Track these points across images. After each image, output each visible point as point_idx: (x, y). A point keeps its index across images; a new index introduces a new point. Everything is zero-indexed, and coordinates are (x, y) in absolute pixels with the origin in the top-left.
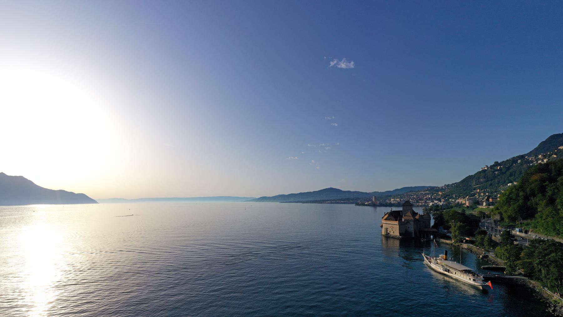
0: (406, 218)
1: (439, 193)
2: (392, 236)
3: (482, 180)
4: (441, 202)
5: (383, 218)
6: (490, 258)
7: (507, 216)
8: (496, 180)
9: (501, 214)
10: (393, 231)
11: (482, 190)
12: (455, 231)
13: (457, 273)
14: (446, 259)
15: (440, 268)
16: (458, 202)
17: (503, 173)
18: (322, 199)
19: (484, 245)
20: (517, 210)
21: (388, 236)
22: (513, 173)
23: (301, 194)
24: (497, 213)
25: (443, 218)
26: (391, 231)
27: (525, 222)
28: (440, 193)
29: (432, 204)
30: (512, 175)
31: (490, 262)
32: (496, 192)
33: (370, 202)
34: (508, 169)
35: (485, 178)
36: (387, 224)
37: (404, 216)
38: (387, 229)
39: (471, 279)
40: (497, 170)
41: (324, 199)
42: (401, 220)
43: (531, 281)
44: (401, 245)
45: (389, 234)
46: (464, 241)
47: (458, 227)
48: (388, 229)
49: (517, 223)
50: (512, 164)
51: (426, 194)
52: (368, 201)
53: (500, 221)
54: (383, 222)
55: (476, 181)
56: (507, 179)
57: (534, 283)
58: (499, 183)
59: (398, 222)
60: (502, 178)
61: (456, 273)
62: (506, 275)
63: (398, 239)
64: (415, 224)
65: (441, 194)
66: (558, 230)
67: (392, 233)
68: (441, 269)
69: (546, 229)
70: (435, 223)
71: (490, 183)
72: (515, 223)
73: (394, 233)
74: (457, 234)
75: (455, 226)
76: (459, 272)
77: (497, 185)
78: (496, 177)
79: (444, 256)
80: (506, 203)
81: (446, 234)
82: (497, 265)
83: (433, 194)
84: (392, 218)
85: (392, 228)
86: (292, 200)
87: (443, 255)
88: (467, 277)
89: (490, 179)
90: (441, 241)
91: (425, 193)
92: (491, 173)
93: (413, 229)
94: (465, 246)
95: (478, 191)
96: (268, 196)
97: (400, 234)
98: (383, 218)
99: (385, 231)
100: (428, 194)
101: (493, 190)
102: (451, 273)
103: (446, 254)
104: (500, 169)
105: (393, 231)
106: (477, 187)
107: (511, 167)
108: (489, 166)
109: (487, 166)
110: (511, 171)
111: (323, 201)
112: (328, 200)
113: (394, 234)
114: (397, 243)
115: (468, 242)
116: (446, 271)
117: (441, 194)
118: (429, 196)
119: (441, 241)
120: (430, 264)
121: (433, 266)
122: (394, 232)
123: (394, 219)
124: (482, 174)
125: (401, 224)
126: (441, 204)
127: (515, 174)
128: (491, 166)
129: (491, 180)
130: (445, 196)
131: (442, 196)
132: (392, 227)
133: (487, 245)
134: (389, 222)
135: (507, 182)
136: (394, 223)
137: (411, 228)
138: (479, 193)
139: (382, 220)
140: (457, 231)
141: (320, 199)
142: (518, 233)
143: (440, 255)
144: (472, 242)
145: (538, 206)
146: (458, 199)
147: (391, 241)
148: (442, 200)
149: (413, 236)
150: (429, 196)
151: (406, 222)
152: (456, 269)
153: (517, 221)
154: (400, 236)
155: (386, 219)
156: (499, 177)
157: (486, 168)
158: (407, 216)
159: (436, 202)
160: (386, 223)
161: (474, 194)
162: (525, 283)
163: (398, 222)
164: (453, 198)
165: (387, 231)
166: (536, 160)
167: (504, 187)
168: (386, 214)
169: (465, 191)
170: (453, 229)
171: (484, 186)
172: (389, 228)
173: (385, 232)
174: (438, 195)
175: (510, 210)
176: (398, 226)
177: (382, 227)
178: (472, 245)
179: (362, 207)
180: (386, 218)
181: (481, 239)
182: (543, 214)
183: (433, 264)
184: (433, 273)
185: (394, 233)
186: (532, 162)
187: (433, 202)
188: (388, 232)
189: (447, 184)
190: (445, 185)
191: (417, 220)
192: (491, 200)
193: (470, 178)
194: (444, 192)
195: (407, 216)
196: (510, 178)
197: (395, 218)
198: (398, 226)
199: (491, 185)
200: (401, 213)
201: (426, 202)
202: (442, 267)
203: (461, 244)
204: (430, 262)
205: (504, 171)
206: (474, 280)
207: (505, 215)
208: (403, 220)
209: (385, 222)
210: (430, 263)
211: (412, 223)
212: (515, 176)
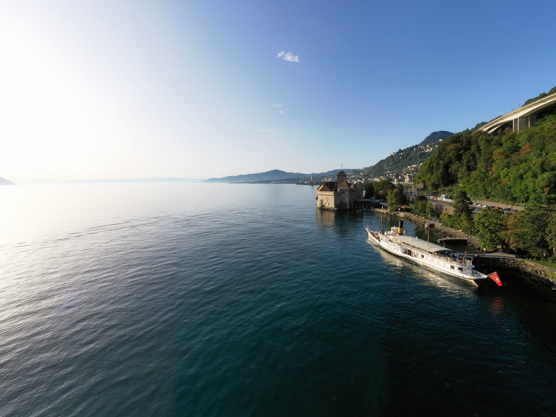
0: (342, 188)
1: (361, 174)
2: (327, 208)
3: (390, 163)
4: (362, 181)
5: (318, 189)
6: (437, 227)
7: (431, 184)
8: (400, 164)
9: (424, 182)
10: (328, 203)
11: (391, 171)
12: (392, 199)
13: (425, 257)
14: (401, 234)
15: (396, 248)
16: (375, 180)
17: (404, 158)
18: (267, 180)
19: (425, 213)
20: (440, 177)
21: (323, 209)
22: (411, 159)
23: (249, 175)
24: (421, 181)
25: (373, 189)
26: (327, 204)
27: (447, 188)
28: (361, 174)
29: (356, 183)
30: (411, 159)
31: (439, 232)
32: (400, 173)
33: (309, 181)
34: (408, 155)
35: (393, 162)
36: (322, 195)
37: (340, 186)
38: (322, 200)
39: (455, 267)
40: (401, 156)
41: (270, 180)
42: (337, 190)
43: (526, 261)
44: (336, 218)
45: (324, 206)
46: (399, 209)
47: (395, 194)
48: (323, 201)
49: (439, 190)
50: (410, 152)
51: (351, 175)
52: (307, 181)
53: (423, 189)
54: (318, 193)
55: (386, 164)
56: (407, 163)
57: (534, 265)
58: (402, 166)
59: (333, 192)
60: (404, 162)
61: (423, 256)
62: (485, 253)
63: (333, 211)
64: (350, 194)
65: (362, 174)
66: (490, 193)
67: (327, 206)
68: (399, 249)
69: (475, 193)
70: (366, 195)
71: (396, 165)
72: (438, 190)
73: (329, 205)
74: (393, 201)
75: (392, 193)
76: (430, 255)
77: (400, 168)
78: (400, 161)
79: (399, 229)
80: (428, 172)
81: (379, 204)
82: (451, 236)
83: (356, 175)
84: (327, 188)
85: (327, 199)
86: (240, 181)
87: (396, 228)
88: (439, 261)
89: (396, 163)
90: (376, 211)
91: (351, 174)
92: (397, 158)
93: (348, 200)
94: (402, 214)
95: (388, 172)
96: (217, 178)
97: (335, 205)
98: (318, 189)
99: (320, 203)
100: (353, 175)
101: (398, 172)
102: (415, 256)
103: (401, 227)
104: (403, 155)
105: (328, 203)
106: (387, 169)
107: (410, 154)
108: (395, 153)
109: (394, 152)
110: (410, 156)
111: (268, 181)
112: (273, 181)
113: (329, 206)
114: (332, 215)
115: (403, 210)
116: (405, 253)
117: (362, 174)
118: (354, 176)
119: (376, 211)
120: (379, 242)
121: (384, 244)
123: (329, 190)
124: (391, 159)
125: (336, 195)
126: (363, 182)
127: (412, 159)
128: (396, 152)
129: (397, 163)
130: (366, 176)
131: (363, 176)
132: (328, 198)
133: (429, 212)
134: (324, 193)
135: (407, 165)
136: (329, 194)
137: (347, 199)
138: (389, 174)
139: (318, 191)
140: (394, 199)
141: (265, 180)
142: (444, 199)
143: (392, 228)
144: (408, 210)
145: (459, 172)
146: (374, 178)
147: (327, 213)
148: (363, 179)
149: (348, 207)
150: (354, 176)
151: (341, 192)
152: (408, 244)
153: (439, 188)
154: (335, 207)
155: (321, 190)
156: (402, 161)
157: (393, 154)
158: (343, 186)
159: (359, 181)
160: (322, 194)
161: (386, 175)
162: (518, 265)
163: (333, 192)
164: (371, 178)
165: (322, 203)
166: (425, 149)
167: (405, 169)
168: (322, 185)
169: (379, 172)
170: (390, 197)
171: (392, 168)
173: (320, 205)
174: (360, 175)
175: (434, 177)
176: (334, 196)
177: (317, 199)
178: (408, 213)
179: (302, 185)
180: (321, 189)
181: (422, 205)
182: (471, 178)
183: (384, 242)
184: (383, 253)
185: (329, 205)
186: (423, 150)
187: (357, 181)
188: (324, 204)
189: (366, 167)
190: (365, 168)
191: (352, 190)
192: (400, 177)
193: (382, 161)
194: (364, 172)
195: (343, 186)
196: (409, 162)
197: (330, 189)
198: (333, 197)
199: (397, 167)
200: (335, 184)
201: (351, 181)
202: (399, 247)
203: (398, 213)
204: (378, 238)
205: (405, 157)
206: (460, 269)
207: (428, 184)
208: (338, 190)
209: (320, 193)
210: (379, 241)
211: (347, 193)
212: (412, 160)
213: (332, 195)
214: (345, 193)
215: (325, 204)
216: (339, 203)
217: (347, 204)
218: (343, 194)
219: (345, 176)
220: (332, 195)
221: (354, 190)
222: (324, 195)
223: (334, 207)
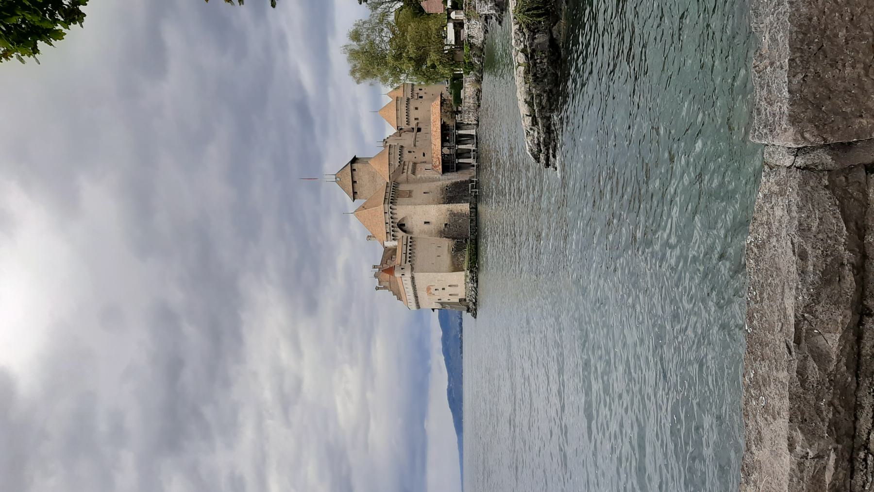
10: (447, 288)
64: (410, 194)
85: (433, 291)
97: (456, 268)
105: (447, 288)
122: (449, 286)
132: (428, 289)
151: (400, 234)
172: (439, 298)
211: (402, 211)
213: (413, 278)
214: (403, 219)
215: (456, 295)
216: (447, 244)
217: (453, 214)
218: (408, 225)
219: (353, 170)
220: (413, 278)
221: (397, 164)
222: (416, 297)
223: (463, 273)
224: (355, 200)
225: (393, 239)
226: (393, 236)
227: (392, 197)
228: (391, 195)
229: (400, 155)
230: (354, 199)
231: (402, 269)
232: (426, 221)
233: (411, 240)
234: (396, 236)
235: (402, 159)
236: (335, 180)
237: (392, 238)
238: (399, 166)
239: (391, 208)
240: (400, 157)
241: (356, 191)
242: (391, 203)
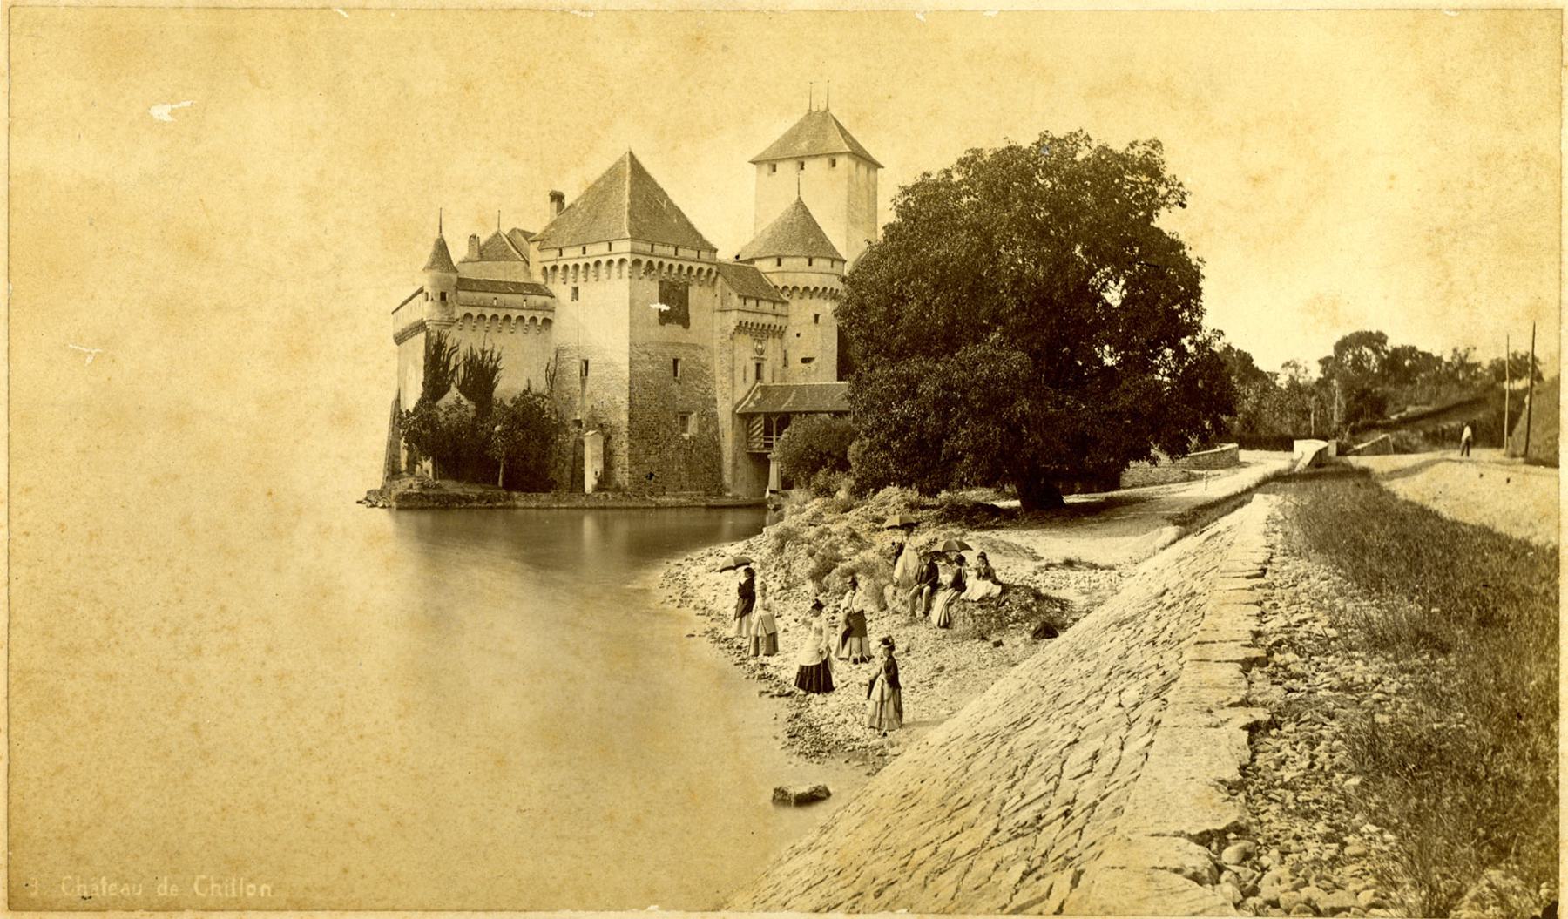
224: (755, 166)
225: (545, 268)
226: (555, 268)
227: (661, 264)
228: (667, 263)
229: (806, 289)
230: (754, 162)
231: (443, 296)
232: (590, 366)
233: (539, 322)
234: (553, 278)
235: (796, 295)
236: (814, 109)
237: (549, 266)
238: (776, 287)
239: (622, 261)
240: (801, 290)
241: (779, 166)
242: (637, 263)
